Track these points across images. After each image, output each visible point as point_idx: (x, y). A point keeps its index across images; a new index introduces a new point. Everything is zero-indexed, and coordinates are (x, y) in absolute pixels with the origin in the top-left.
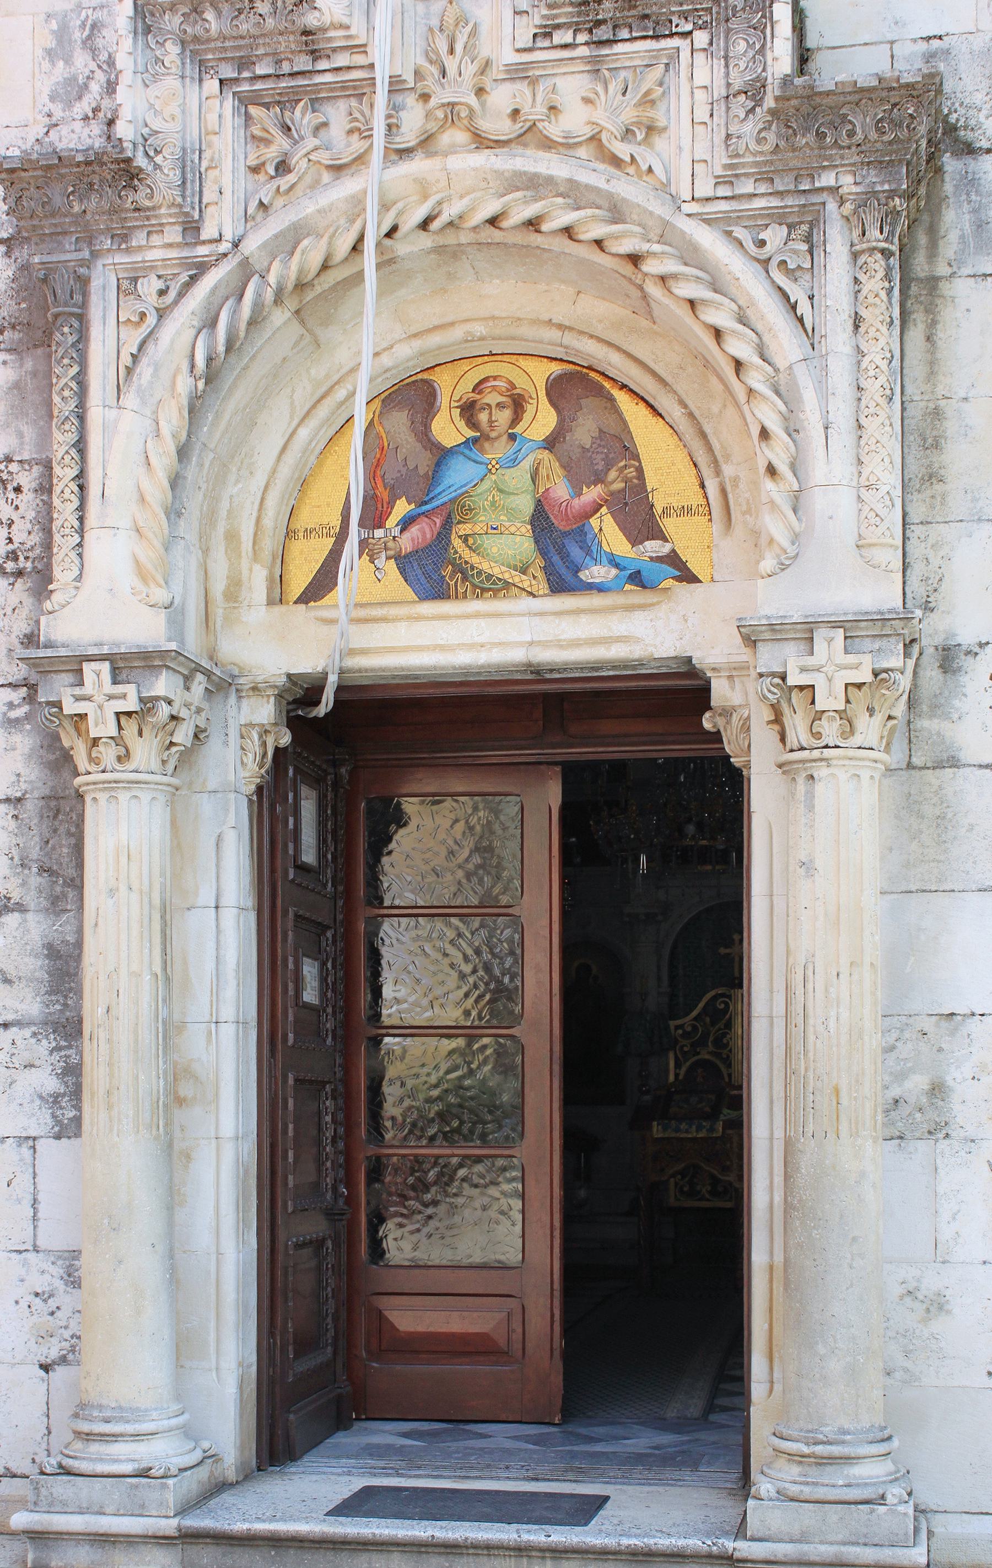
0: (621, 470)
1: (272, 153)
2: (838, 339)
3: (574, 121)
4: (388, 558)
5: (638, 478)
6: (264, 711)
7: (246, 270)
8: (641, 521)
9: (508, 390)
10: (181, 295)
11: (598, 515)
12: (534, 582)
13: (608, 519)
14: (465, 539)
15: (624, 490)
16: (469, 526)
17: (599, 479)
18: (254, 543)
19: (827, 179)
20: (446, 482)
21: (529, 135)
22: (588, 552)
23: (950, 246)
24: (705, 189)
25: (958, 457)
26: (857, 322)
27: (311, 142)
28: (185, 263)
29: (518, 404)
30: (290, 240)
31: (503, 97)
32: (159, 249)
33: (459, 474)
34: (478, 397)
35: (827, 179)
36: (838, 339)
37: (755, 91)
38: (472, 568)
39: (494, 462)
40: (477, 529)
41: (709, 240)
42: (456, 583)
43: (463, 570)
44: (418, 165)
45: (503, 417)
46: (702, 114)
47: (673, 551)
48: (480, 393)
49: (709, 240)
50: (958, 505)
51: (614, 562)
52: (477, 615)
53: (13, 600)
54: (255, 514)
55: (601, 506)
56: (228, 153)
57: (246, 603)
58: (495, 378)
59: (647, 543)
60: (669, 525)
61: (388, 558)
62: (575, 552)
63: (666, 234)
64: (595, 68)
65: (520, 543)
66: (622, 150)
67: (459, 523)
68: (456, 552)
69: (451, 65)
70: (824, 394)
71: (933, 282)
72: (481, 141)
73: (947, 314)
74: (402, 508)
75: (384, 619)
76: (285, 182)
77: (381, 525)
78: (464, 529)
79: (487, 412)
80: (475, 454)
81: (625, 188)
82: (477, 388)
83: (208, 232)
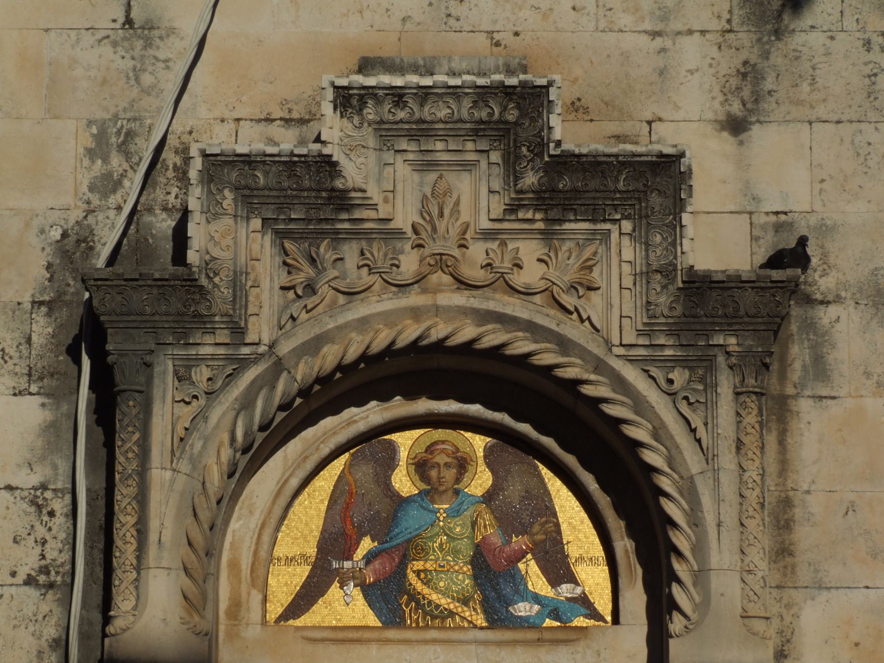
0: (543, 525)
1: (299, 278)
2: (727, 460)
3: (531, 275)
4: (355, 586)
5: (555, 532)
7: (279, 367)
8: (559, 569)
9: (454, 453)
10: (226, 385)
11: (524, 560)
12: (473, 613)
13: (533, 562)
14: (418, 573)
15: (544, 541)
16: (422, 563)
17: (524, 530)
18: (252, 571)
19: (719, 339)
20: (404, 524)
22: (517, 592)
23: (796, 372)
24: (629, 339)
25: (804, 536)
26: (739, 445)
27: (332, 273)
28: (229, 359)
29: (462, 464)
30: (313, 346)
31: (478, 251)
32: (208, 346)
33: (412, 520)
34: (430, 456)
35: (719, 339)
36: (727, 460)
37: (668, 271)
38: (424, 598)
39: (442, 511)
40: (428, 565)
41: (631, 374)
42: (410, 610)
43: (414, 597)
45: (449, 474)
46: (628, 282)
47: (584, 593)
48: (432, 453)
49: (631, 374)
50: (804, 575)
51: (537, 599)
52: (434, 641)
53: (45, 608)
54: (253, 548)
55: (527, 553)
57: (244, 621)
58: (443, 442)
59: (564, 586)
60: (582, 572)
61: (355, 586)
62: (508, 590)
63: (600, 366)
64: (548, 236)
65: (464, 581)
66: (568, 300)
67: (414, 560)
68: (411, 584)
69: (441, 226)
70: (718, 500)
72: (463, 284)
73: (793, 424)
74: (366, 545)
75: (359, 641)
76: (310, 302)
77: (349, 558)
78: (418, 565)
79: (436, 470)
80: (426, 503)
81: (572, 330)
82: (430, 449)
83: (251, 337)
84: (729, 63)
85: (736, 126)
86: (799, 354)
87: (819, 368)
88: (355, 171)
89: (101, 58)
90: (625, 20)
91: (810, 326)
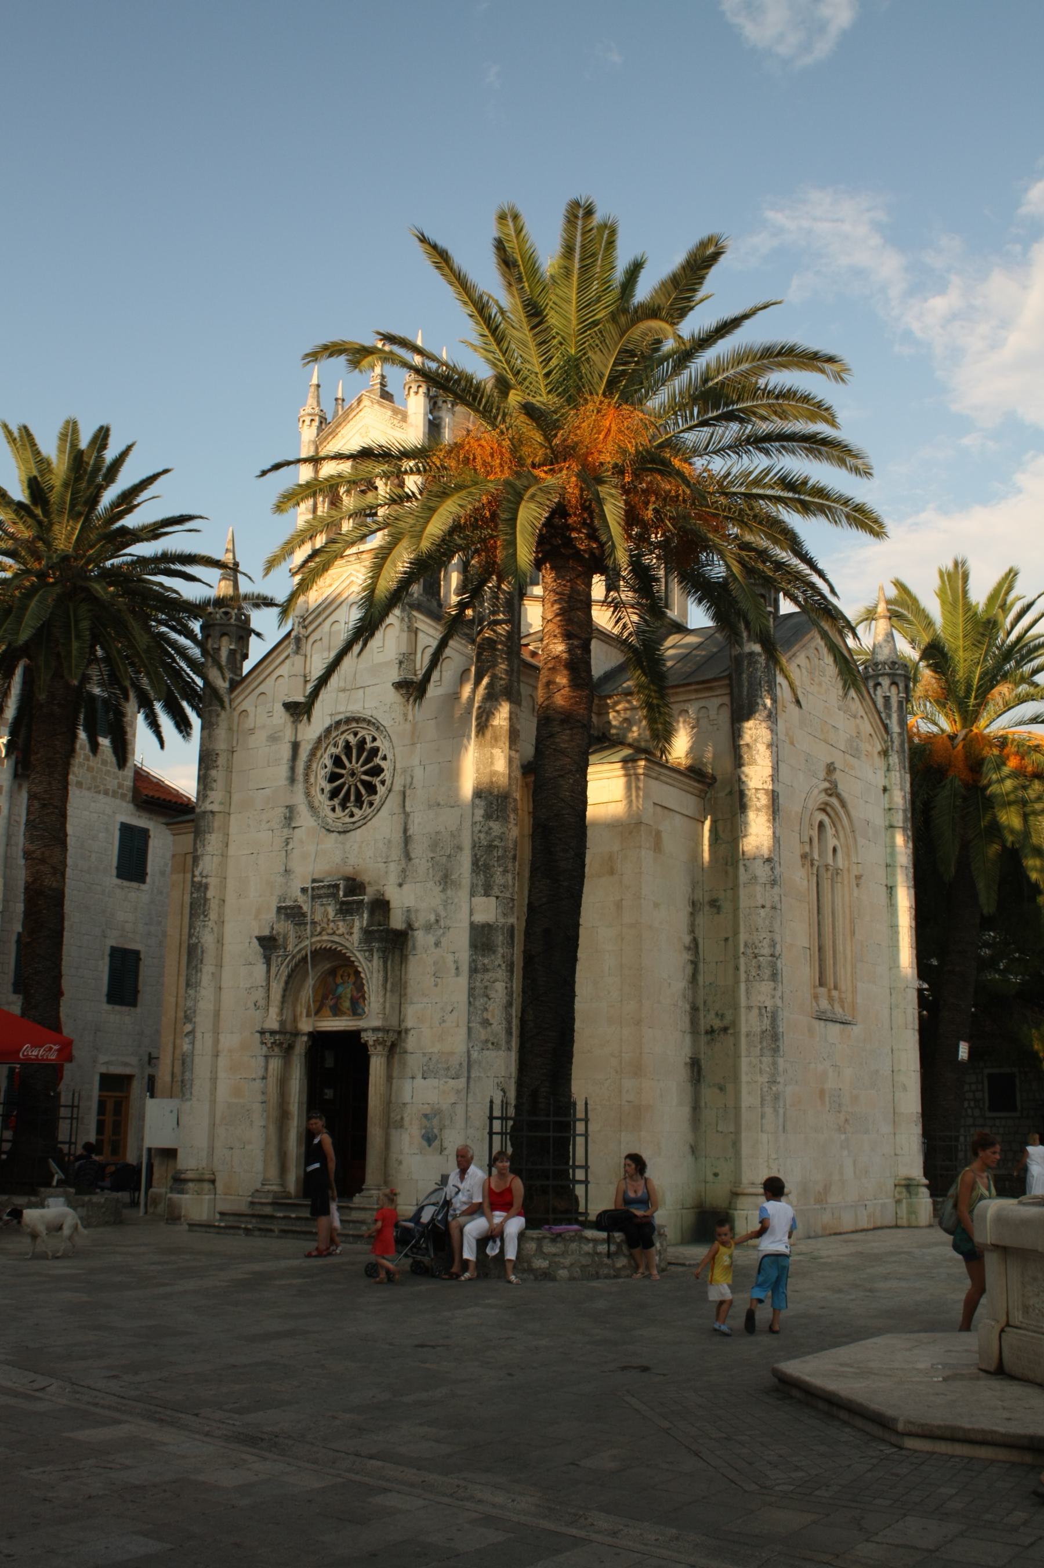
3: (341, 931)
6: (305, 1038)
7: (294, 957)
21: (334, 933)
31: (332, 925)
44: (318, 938)
56: (292, 934)
71: (406, 956)
81: (347, 944)
84: (400, 868)
85: (400, 885)
86: (410, 944)
87: (414, 948)
88: (306, 908)
89: (280, 880)
90: (379, 860)
91: (413, 936)
